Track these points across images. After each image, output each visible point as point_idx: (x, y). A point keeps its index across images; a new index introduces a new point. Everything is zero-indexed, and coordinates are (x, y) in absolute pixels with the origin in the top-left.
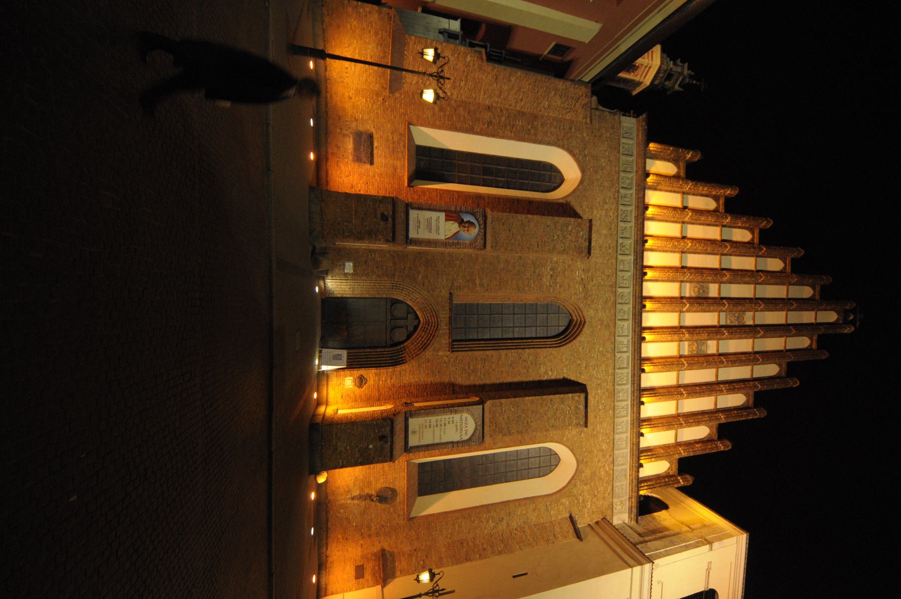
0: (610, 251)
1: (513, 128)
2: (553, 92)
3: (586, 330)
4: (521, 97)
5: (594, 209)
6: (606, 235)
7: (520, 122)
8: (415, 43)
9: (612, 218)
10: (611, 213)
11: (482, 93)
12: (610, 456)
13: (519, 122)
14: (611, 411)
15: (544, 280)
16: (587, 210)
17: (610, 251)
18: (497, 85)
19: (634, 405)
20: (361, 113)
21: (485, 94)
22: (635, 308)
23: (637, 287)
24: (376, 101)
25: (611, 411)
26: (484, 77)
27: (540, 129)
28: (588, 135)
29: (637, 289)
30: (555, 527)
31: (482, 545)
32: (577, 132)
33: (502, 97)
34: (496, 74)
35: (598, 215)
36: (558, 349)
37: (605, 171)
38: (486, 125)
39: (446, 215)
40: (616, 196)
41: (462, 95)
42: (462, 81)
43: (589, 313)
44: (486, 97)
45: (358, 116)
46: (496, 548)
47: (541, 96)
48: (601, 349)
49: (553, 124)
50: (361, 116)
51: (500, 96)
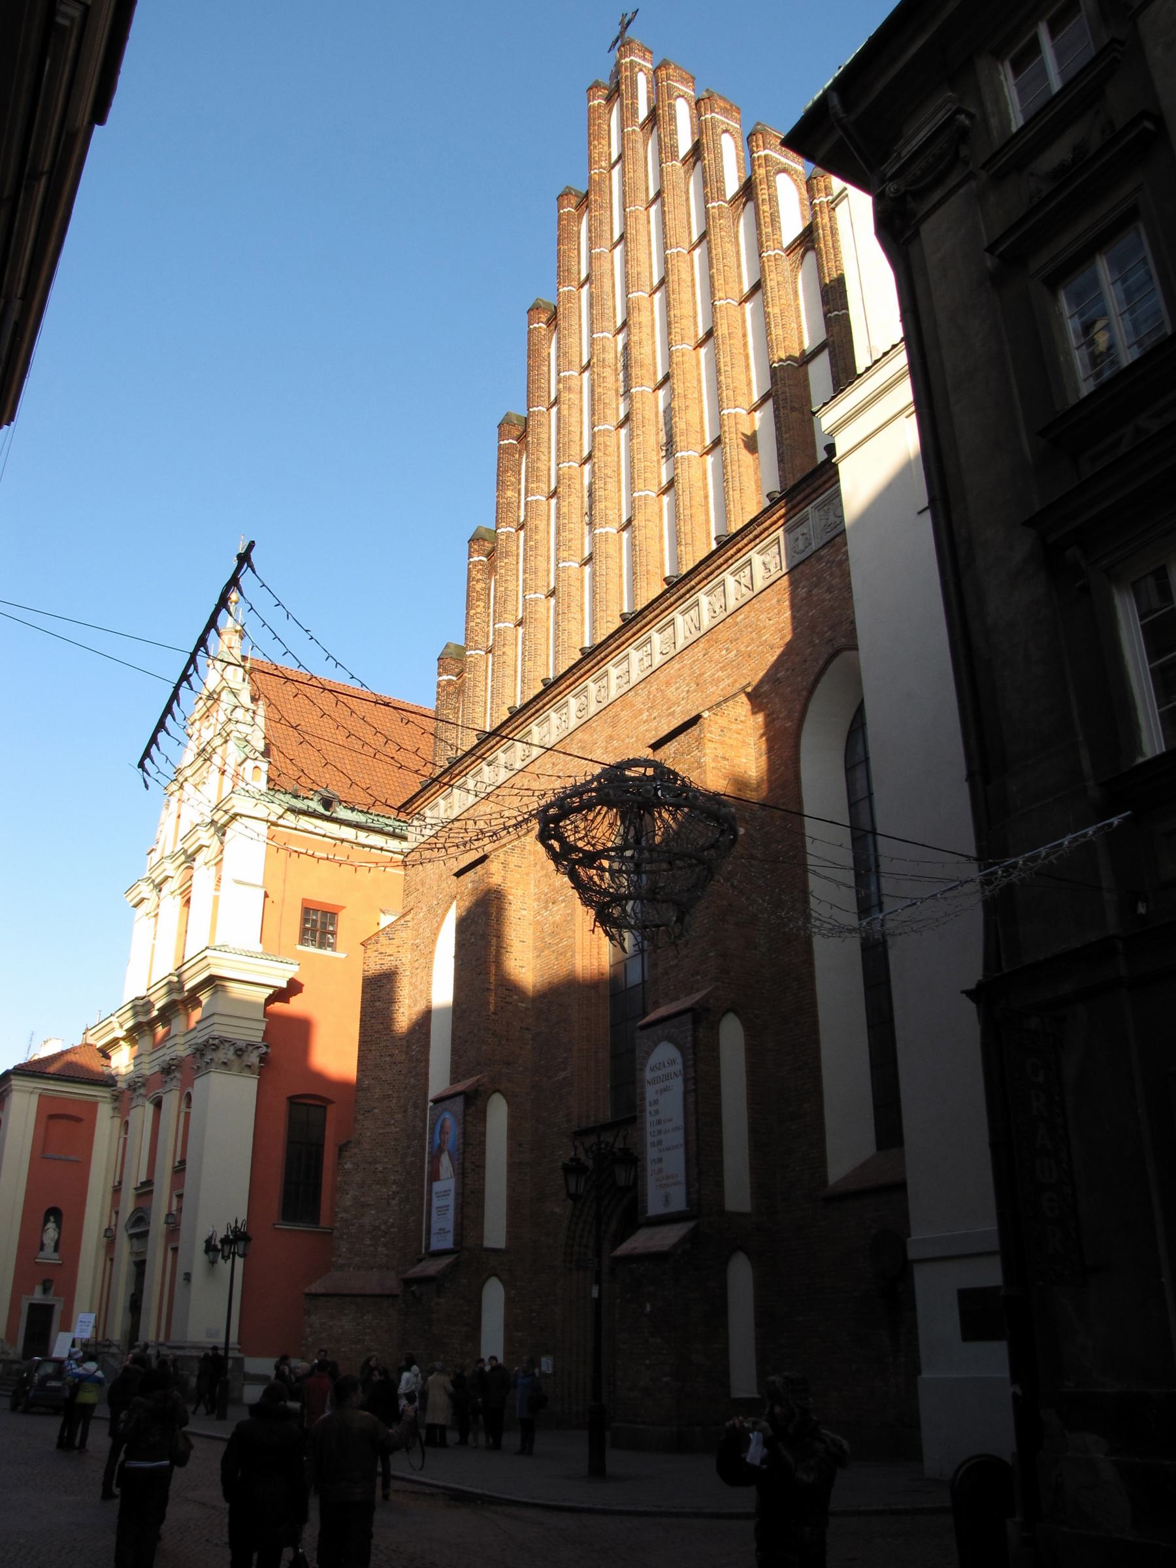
2: (377, 1004)
4: (388, 1059)
8: (340, 1256)
11: (388, 1130)
12: (819, 559)
15: (558, 918)
18: (376, 1108)
19: (726, 561)
21: (389, 1125)
23: (562, 688)
26: (369, 1134)
29: (564, 686)
33: (390, 1092)
34: (364, 1114)
39: (435, 1181)
41: (394, 1165)
42: (376, 1169)
44: (393, 1122)
47: (382, 1023)
48: (645, 716)
51: (389, 1096)
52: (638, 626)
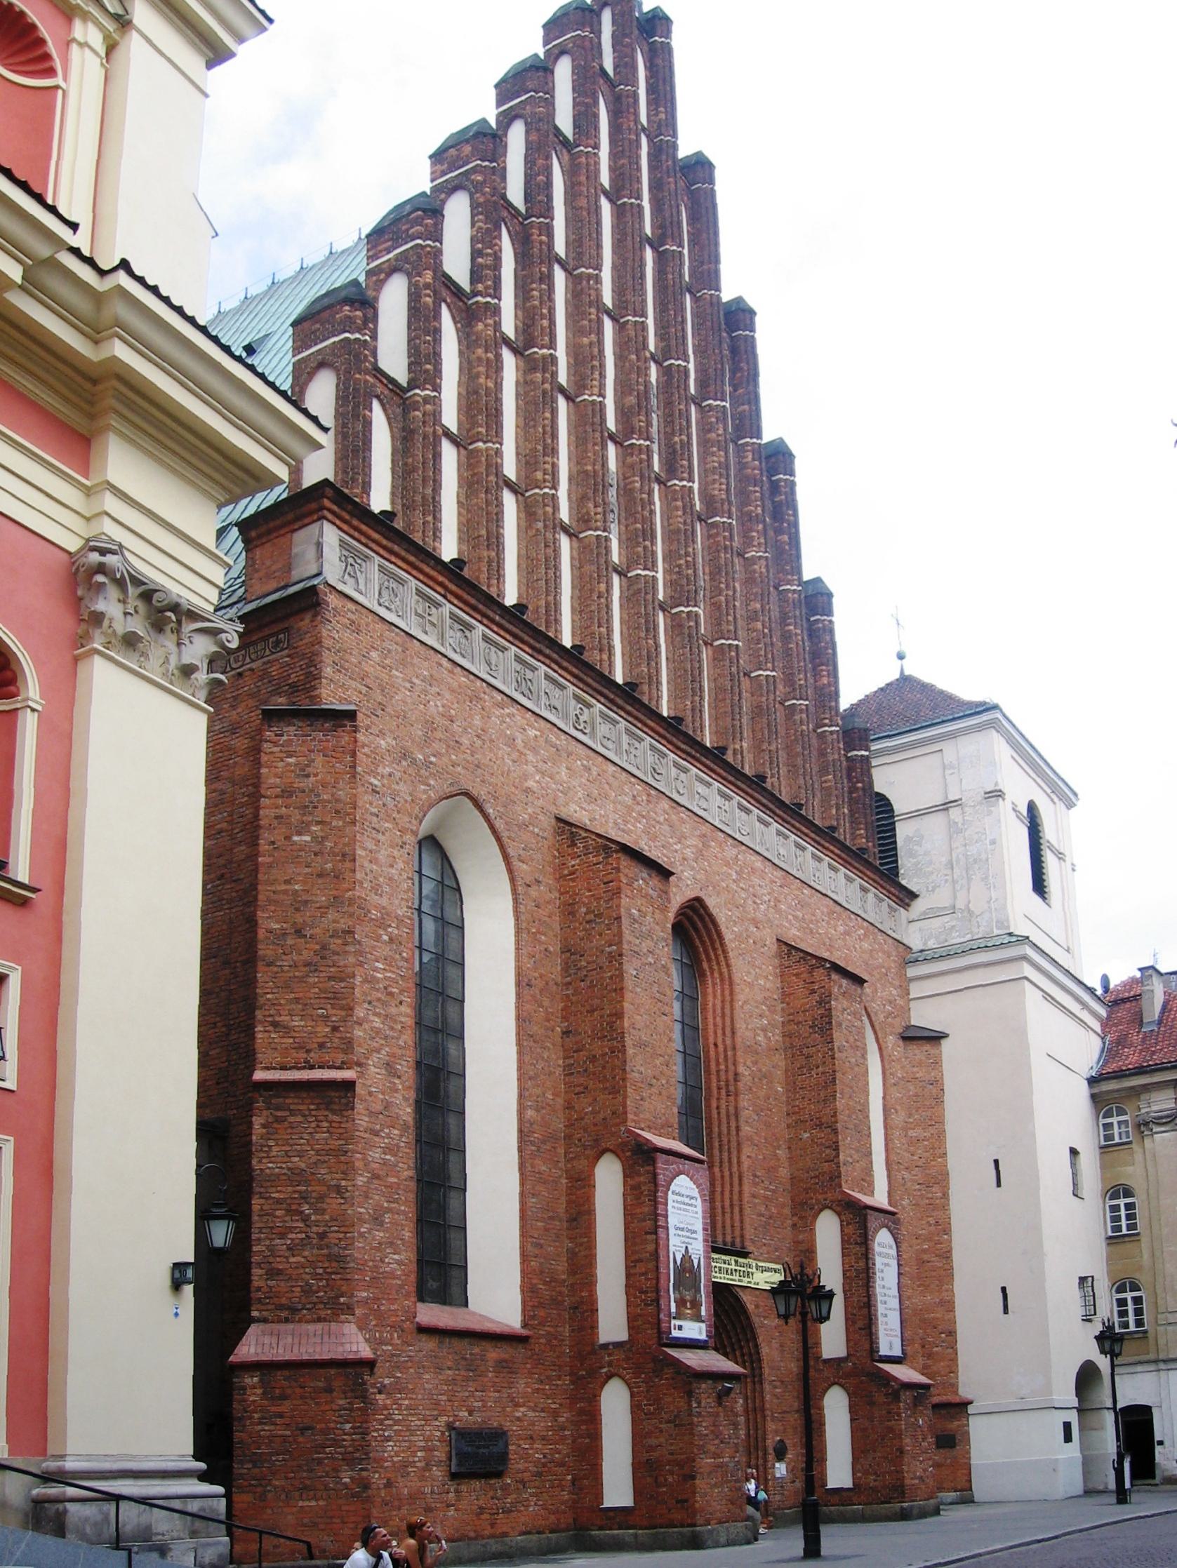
0: (595, 771)
1: (391, 994)
3: (711, 902)
5: (526, 784)
6: (568, 768)
7: (377, 964)
9: (538, 733)
10: (532, 733)
13: (376, 970)
14: (805, 891)
16: (530, 810)
17: (595, 771)
20: (414, 1454)
22: (678, 748)
24: (385, 1412)
25: (805, 891)
27: (384, 901)
28: (382, 734)
30: (918, 1075)
31: (930, 1225)
32: (380, 770)
35: (537, 778)
36: (737, 989)
37: (453, 712)
38: (397, 1081)
40: (499, 697)
43: (689, 882)
45: (420, 1461)
46: (938, 1201)
49: (371, 851)
50: (419, 1454)
52: (760, 798)
